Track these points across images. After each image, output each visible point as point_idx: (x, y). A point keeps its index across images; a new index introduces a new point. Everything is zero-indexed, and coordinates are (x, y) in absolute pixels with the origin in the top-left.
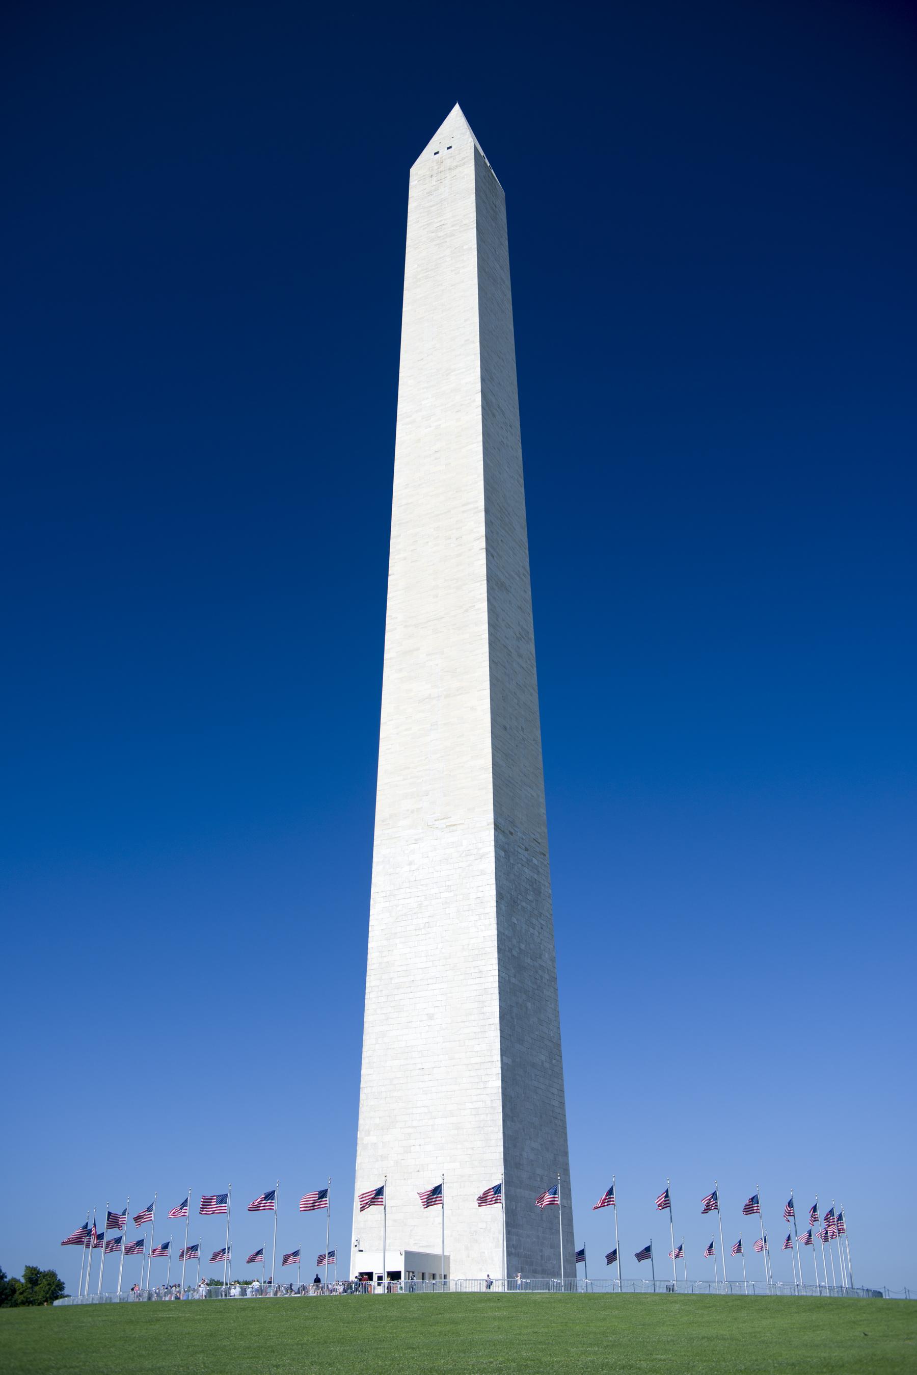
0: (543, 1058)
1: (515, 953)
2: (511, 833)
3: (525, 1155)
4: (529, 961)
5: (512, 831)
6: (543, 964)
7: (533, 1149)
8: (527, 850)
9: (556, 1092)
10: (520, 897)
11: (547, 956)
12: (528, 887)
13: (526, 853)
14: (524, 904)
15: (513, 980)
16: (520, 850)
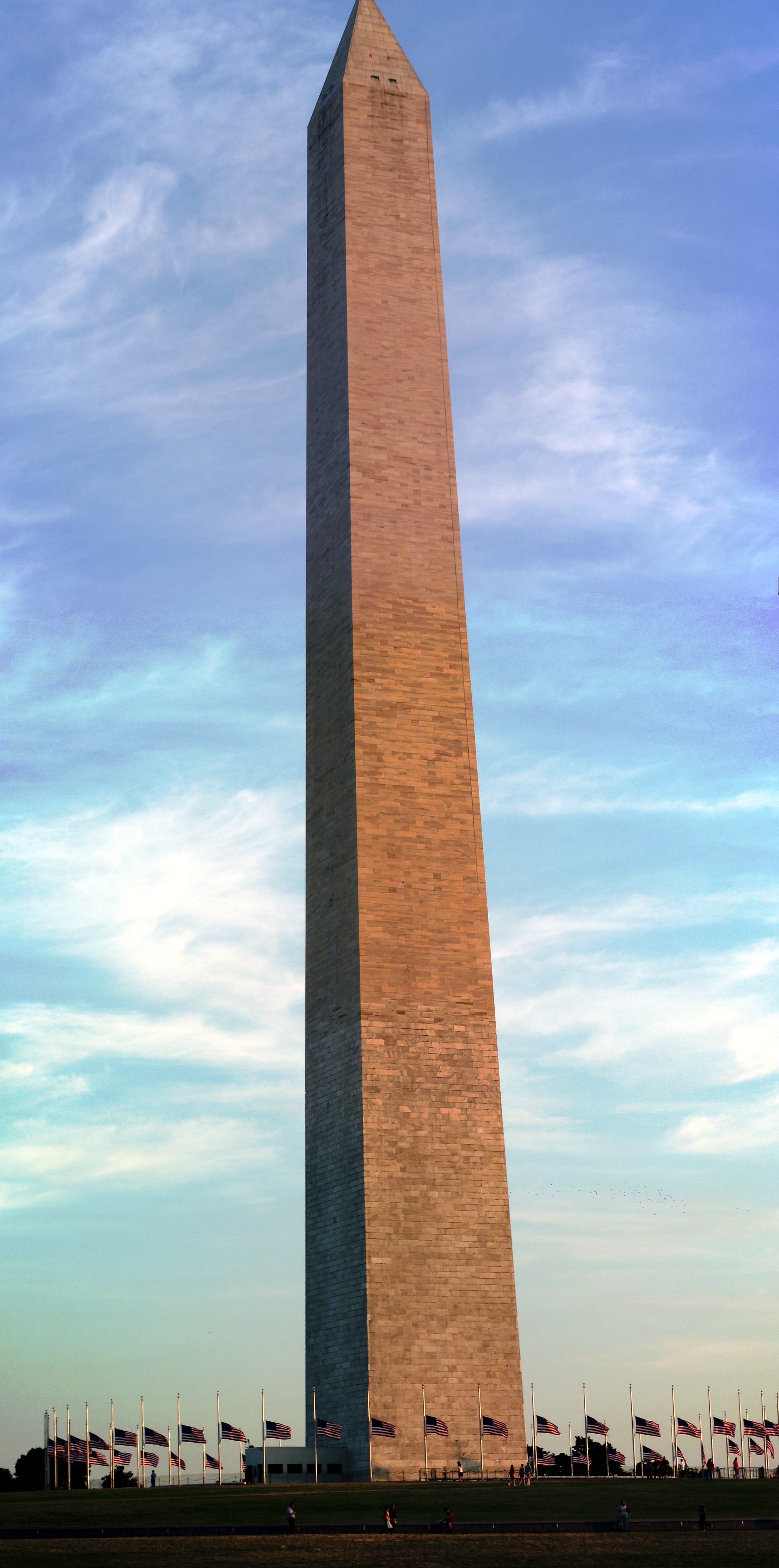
0: (465, 1245)
1: (401, 1144)
2: (402, 1013)
3: (415, 1348)
4: (437, 1146)
5: (402, 1008)
6: (472, 1142)
7: (435, 1341)
8: (437, 1020)
9: (492, 1275)
10: (418, 1080)
11: (481, 1130)
12: (440, 1063)
13: (437, 1027)
14: (429, 1085)
15: (400, 1174)
16: (421, 1026)
